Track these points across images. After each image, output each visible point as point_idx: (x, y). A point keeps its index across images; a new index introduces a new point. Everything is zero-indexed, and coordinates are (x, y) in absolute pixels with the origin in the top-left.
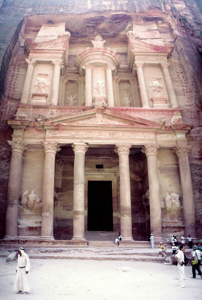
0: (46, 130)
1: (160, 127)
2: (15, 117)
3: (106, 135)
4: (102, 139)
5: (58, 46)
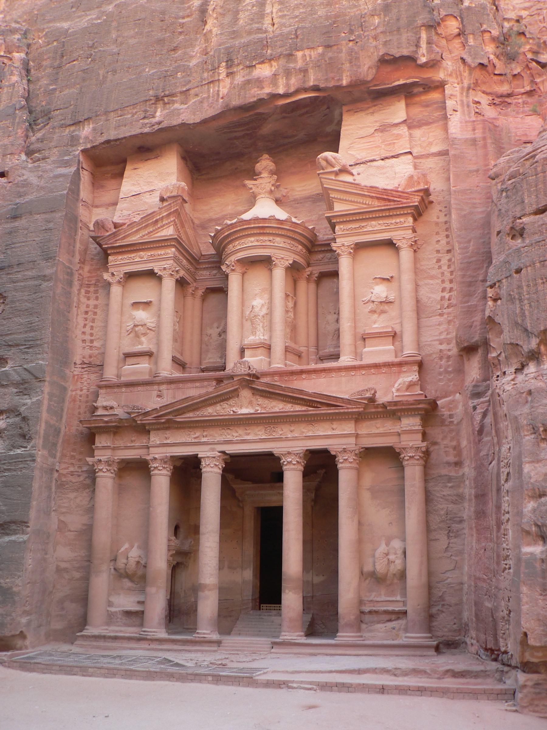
0: (149, 432)
1: (362, 409)
2: (96, 408)
3: (260, 433)
4: (250, 442)
5: (164, 225)
